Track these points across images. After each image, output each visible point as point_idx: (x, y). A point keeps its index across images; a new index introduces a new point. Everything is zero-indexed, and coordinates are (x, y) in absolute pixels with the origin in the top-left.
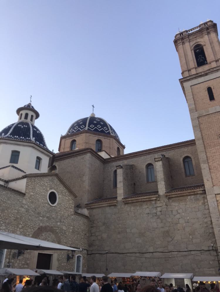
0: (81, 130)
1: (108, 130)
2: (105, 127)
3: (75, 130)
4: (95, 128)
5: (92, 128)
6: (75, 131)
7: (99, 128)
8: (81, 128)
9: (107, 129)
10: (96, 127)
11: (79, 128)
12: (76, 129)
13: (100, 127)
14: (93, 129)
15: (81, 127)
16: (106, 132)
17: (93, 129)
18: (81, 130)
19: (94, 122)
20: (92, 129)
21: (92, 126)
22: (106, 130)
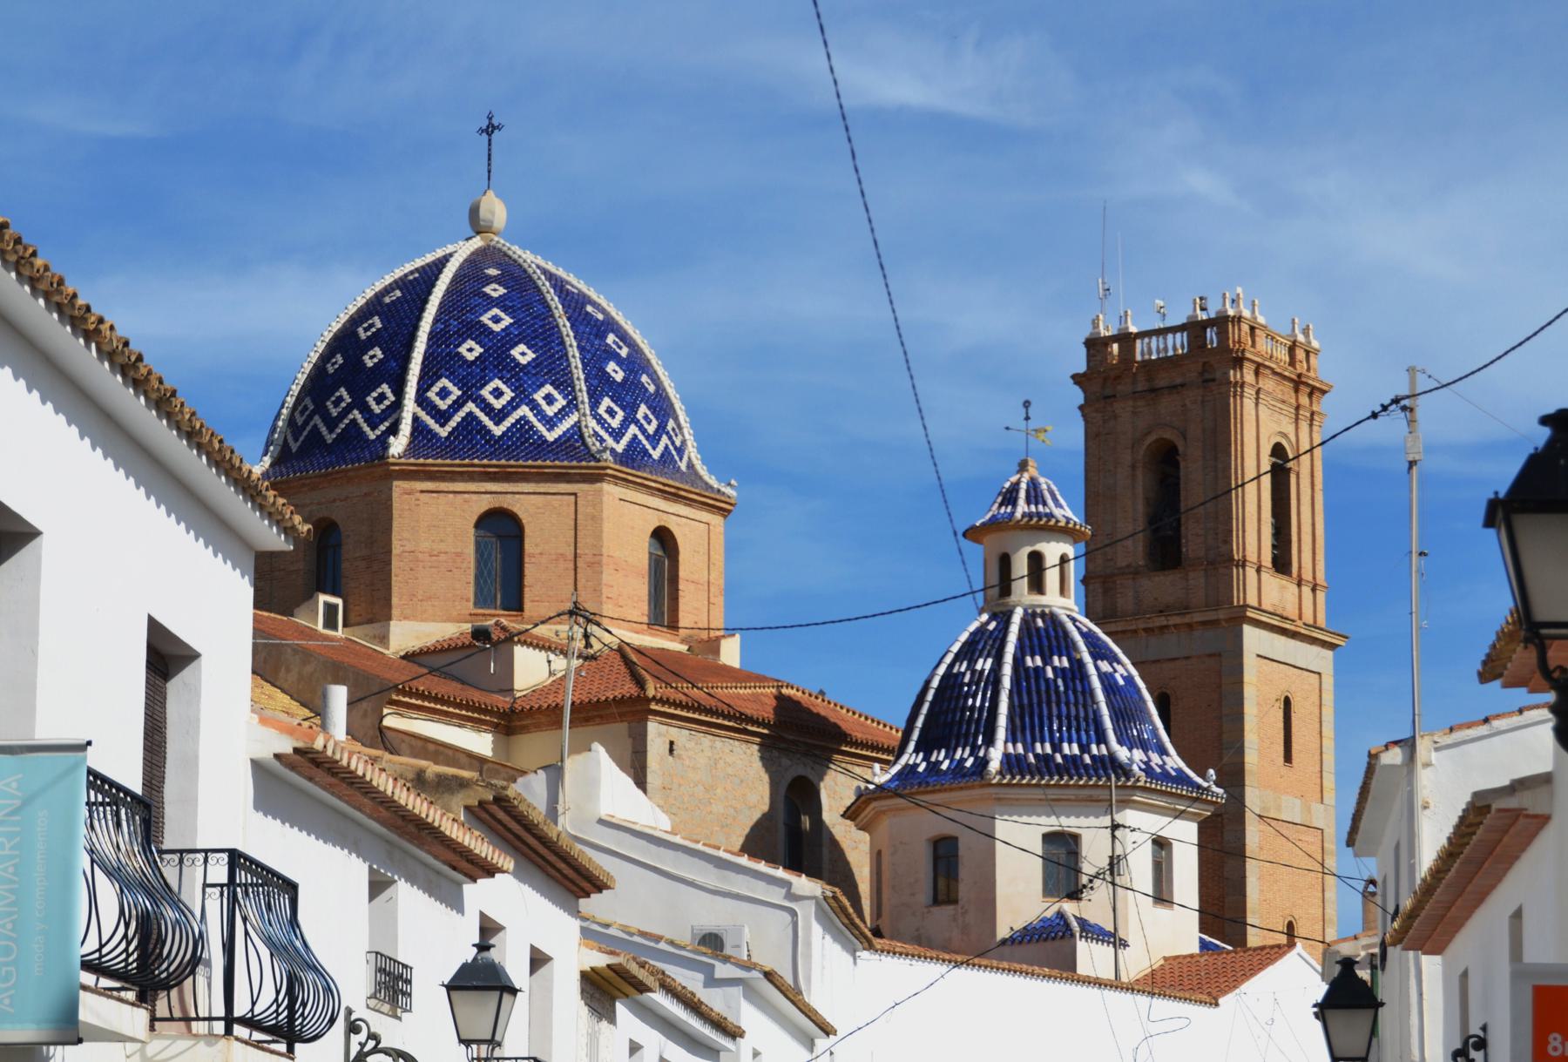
0: (366, 429)
1: (572, 405)
2: (548, 389)
3: (331, 423)
4: (462, 413)
5: (442, 417)
6: (330, 438)
7: (498, 404)
8: (365, 409)
9: (561, 402)
10: (470, 406)
11: (356, 414)
12: (334, 412)
13: (508, 394)
14: (453, 423)
15: (370, 400)
16: (551, 436)
17: (453, 423)
18: (366, 429)
19: (463, 350)
20: (442, 425)
21: (444, 393)
22: (550, 411)
